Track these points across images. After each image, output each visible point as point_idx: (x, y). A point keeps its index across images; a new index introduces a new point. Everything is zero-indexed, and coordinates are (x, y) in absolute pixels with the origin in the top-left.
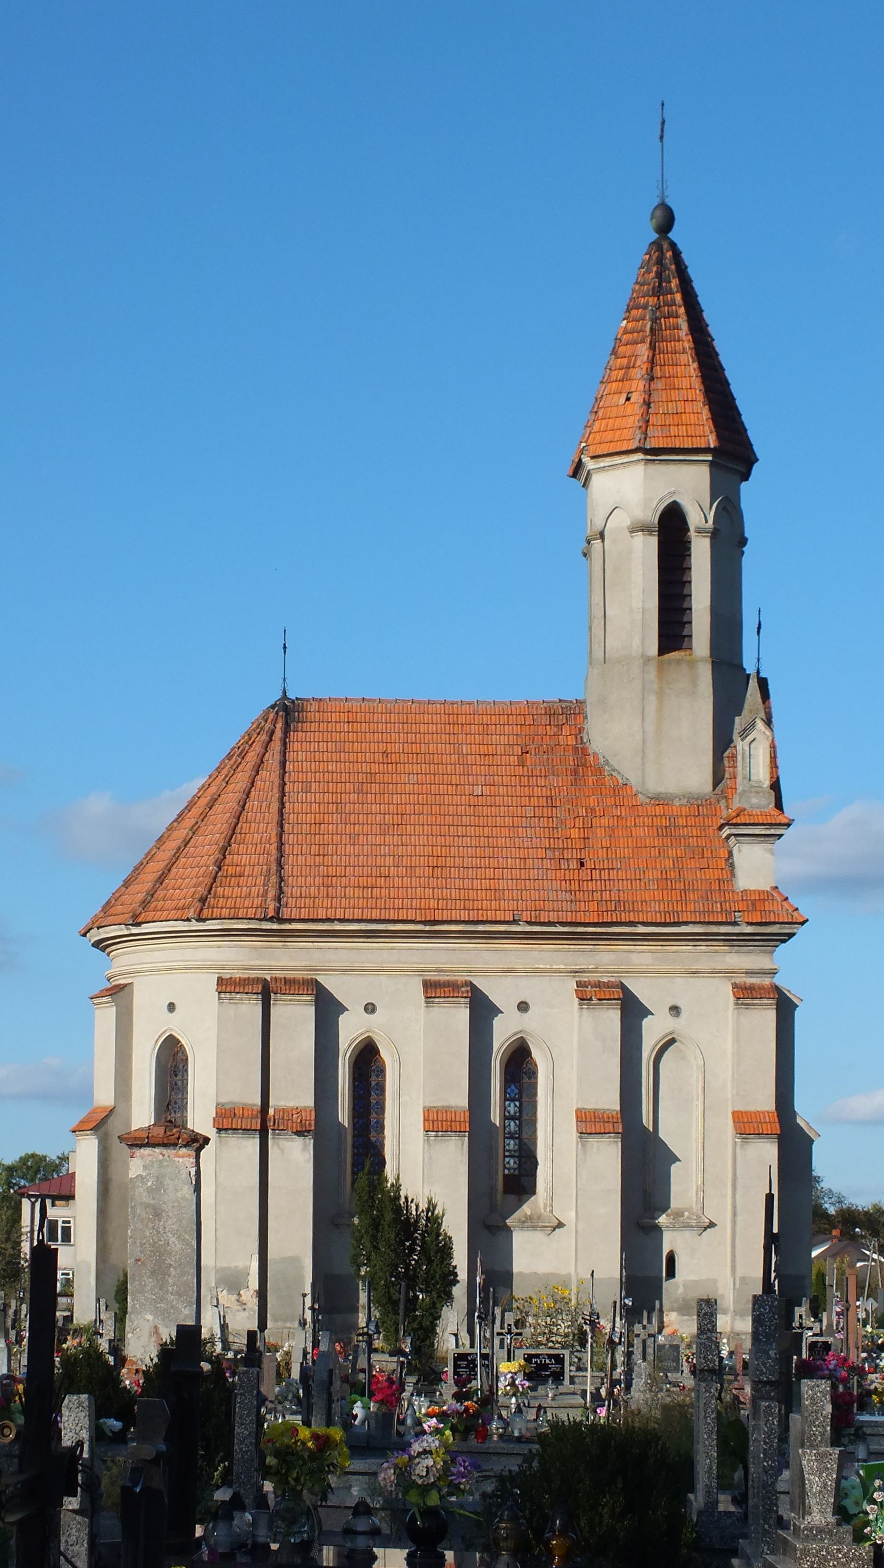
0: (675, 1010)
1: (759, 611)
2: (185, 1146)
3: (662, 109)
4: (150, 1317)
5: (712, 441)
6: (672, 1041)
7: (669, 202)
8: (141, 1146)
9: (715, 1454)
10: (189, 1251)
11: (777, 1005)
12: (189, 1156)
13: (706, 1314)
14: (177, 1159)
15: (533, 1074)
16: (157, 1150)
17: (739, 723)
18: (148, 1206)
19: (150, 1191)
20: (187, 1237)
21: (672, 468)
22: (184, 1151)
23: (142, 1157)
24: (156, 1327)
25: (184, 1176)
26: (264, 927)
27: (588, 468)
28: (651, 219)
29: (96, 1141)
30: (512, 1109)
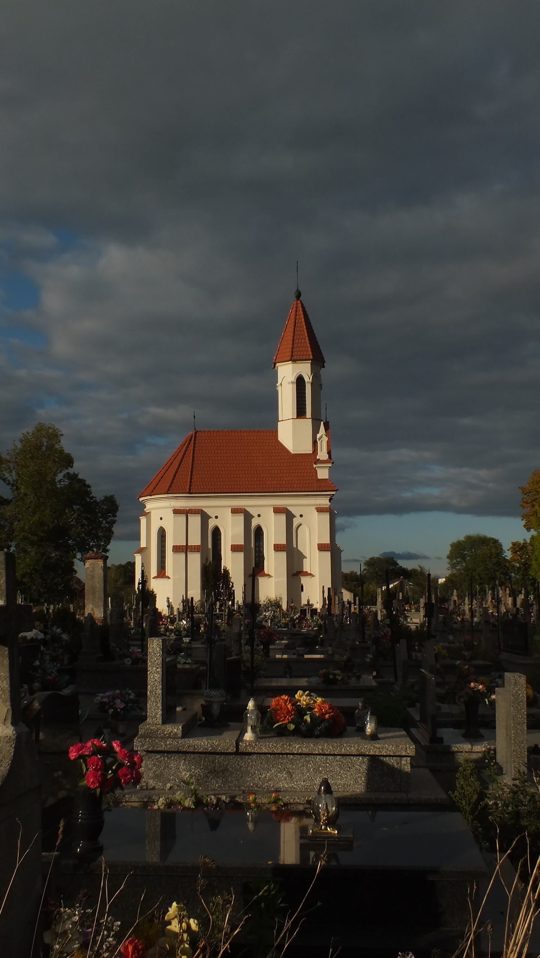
0: (301, 516)
4: (91, 606)
5: (311, 357)
6: (301, 525)
7: (300, 289)
8: (88, 559)
15: (263, 534)
16: (93, 560)
17: (318, 436)
18: (90, 575)
19: (91, 571)
21: (301, 364)
22: (100, 560)
23: (89, 562)
24: (93, 609)
25: (100, 567)
28: (295, 294)
29: (141, 557)
30: (257, 544)
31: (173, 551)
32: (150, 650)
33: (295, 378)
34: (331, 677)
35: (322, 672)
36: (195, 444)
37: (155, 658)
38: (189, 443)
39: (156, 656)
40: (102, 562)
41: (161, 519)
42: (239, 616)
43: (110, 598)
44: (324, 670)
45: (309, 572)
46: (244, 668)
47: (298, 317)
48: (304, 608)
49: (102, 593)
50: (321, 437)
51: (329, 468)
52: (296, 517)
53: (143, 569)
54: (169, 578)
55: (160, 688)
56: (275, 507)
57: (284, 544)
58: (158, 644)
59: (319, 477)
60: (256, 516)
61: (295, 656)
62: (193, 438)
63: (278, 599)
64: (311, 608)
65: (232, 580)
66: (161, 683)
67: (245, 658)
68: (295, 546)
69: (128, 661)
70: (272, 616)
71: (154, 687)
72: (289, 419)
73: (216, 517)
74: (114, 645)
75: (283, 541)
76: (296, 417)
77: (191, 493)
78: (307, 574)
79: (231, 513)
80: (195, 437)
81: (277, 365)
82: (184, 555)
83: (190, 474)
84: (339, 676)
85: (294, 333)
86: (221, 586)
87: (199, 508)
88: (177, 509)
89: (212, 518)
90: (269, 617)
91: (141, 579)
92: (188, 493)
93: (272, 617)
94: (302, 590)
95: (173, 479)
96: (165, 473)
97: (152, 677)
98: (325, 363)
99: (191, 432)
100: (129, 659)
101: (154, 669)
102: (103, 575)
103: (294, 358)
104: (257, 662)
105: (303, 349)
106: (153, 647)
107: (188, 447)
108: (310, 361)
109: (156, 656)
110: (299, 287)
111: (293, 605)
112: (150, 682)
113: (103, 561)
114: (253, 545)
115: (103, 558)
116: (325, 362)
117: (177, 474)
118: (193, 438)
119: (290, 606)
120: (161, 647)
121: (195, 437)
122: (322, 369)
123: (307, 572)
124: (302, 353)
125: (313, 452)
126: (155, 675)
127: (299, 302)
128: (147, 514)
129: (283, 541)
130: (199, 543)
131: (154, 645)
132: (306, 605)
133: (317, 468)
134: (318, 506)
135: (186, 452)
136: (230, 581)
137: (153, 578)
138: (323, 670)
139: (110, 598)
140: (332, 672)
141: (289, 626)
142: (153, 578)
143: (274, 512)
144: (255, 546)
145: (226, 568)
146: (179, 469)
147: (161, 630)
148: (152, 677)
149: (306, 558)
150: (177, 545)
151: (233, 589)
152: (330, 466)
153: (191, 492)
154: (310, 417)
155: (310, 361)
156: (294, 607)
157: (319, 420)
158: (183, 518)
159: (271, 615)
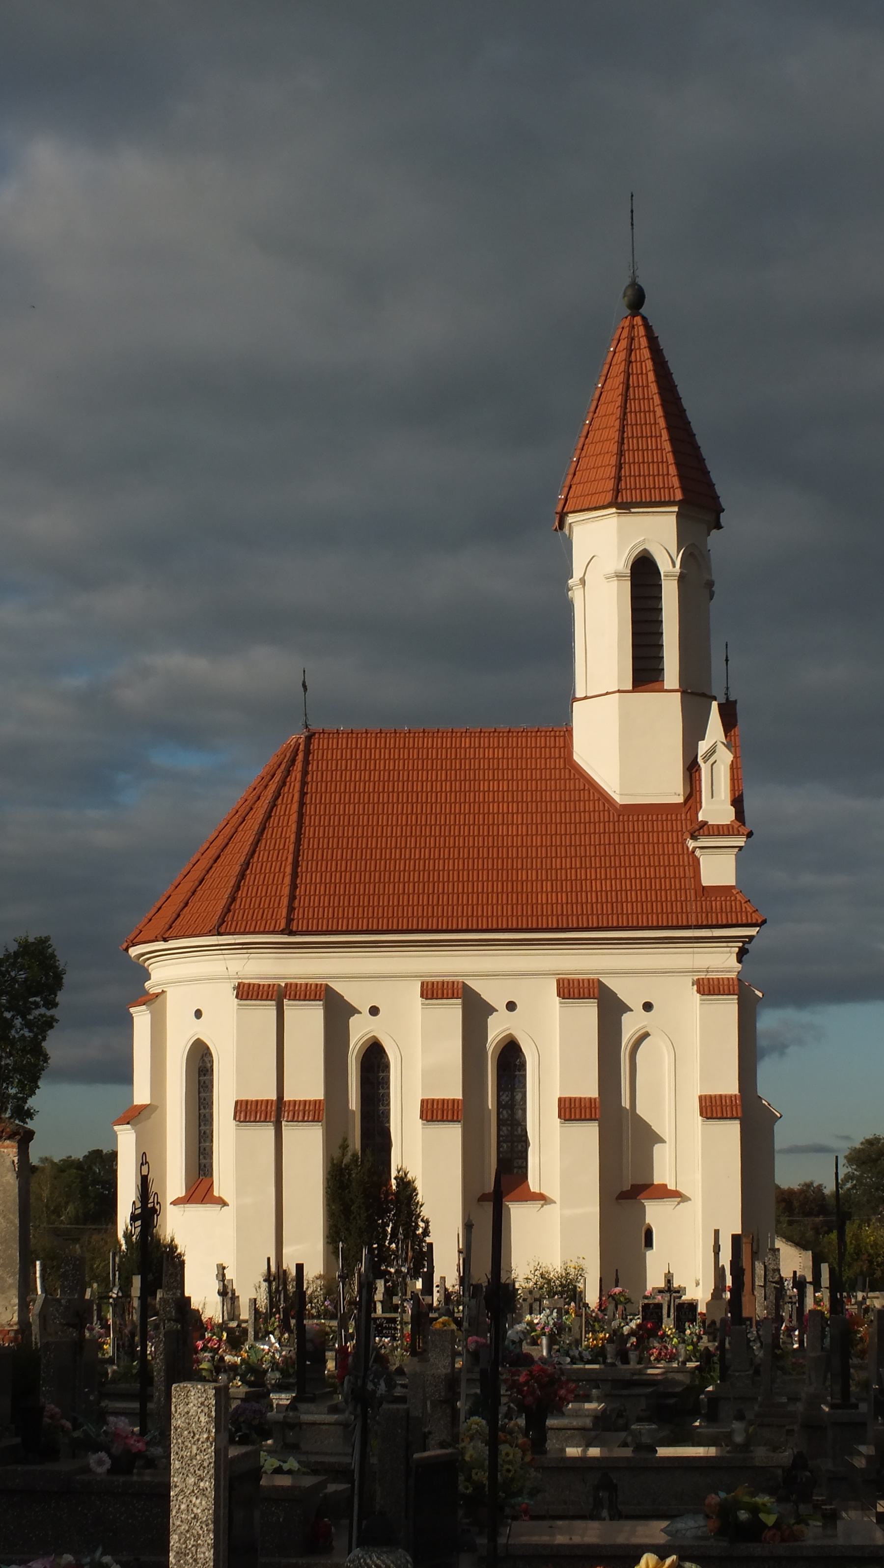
0: (648, 1007)
1: (727, 645)
2: (9, 1138)
3: (632, 199)
5: (679, 496)
6: (646, 1035)
7: (641, 282)
9: (163, 1388)
10: (13, 1228)
11: (738, 999)
12: (13, 1147)
13: (171, 1275)
14: (2, 1150)
15: (523, 1066)
17: (703, 747)
20: (11, 1216)
22: (8, 1142)
25: (8, 1163)
26: (238, 941)
27: (570, 521)
28: (624, 297)
29: (134, 1135)
30: (505, 1098)
31: (235, 1118)
32: (177, 1421)
33: (627, 560)
34: (743, 1515)
35: (713, 1499)
36: (305, 773)
37: (195, 1447)
38: (288, 772)
39: (198, 1440)
40: (15, 1150)
41: (198, 1014)
42: (450, 1325)
43: (38, 1263)
44: (723, 1495)
45: (671, 1187)
46: (467, 1488)
47: (635, 369)
48: (656, 1301)
49: (16, 1246)
50: (712, 751)
51: (737, 850)
52: (632, 1010)
53: (145, 1173)
54: (224, 1204)
55: (209, 1541)
56: (563, 980)
57: (590, 1099)
58: (202, 1404)
59: (705, 883)
60: (499, 1004)
61: (628, 1452)
62: (301, 756)
63: (572, 1271)
64: (678, 1301)
65: (425, 1212)
66: (211, 1526)
67: (471, 1456)
68: (626, 1103)
69: (100, 1462)
70: (555, 1324)
71: (189, 1539)
72: (607, 693)
73: (374, 1011)
74: (57, 1410)
75: (589, 1089)
76: (631, 688)
77: (291, 933)
78: (664, 1193)
79: (422, 996)
80: (307, 752)
81: (571, 519)
82: (269, 1131)
83: (289, 870)
84: (769, 1512)
85: (623, 418)
86: (389, 1230)
87: (319, 981)
88: (249, 984)
89: (360, 1013)
90: (543, 1328)
91: (139, 1205)
92: (282, 932)
93: (552, 1329)
94: (649, 1243)
95: (237, 888)
96: (211, 868)
97: (183, 1507)
98: (721, 514)
99: (296, 736)
100: (103, 1455)
101: (191, 1480)
102: (17, 1190)
103: (625, 497)
104: (507, 1466)
105: (654, 470)
106: (188, 1413)
107: (284, 784)
108: (676, 509)
109: (198, 1440)
110: (637, 273)
111: (617, 1290)
112: (179, 1523)
113: (16, 1144)
114: (491, 1102)
115: (18, 1137)
116: (723, 510)
117: (248, 872)
118: (301, 756)
119: (610, 1296)
120: (213, 1414)
121: (307, 752)
122: (714, 532)
123: (666, 1185)
124: (649, 482)
125: (687, 800)
126: (194, 1499)
127: (638, 320)
128: (152, 1000)
129: (589, 1089)
130: (318, 1093)
131: (192, 1405)
132: (661, 1291)
133: (698, 853)
134: (702, 976)
135: (277, 798)
136: (419, 1216)
137: (171, 1204)
138: (717, 1494)
139: (38, 1263)
140: (746, 1499)
141: (608, 1356)
142: (174, 1203)
143: (559, 995)
144: (500, 1105)
145: (406, 1175)
146: (256, 855)
147: (201, 1367)
148: (183, 1507)
149: (663, 1141)
150: (250, 1098)
151: (428, 1239)
152: (742, 844)
153: (294, 929)
154: (677, 687)
155: (676, 509)
156: (622, 1299)
157: (704, 695)
158: (267, 1012)
159: (551, 1322)
